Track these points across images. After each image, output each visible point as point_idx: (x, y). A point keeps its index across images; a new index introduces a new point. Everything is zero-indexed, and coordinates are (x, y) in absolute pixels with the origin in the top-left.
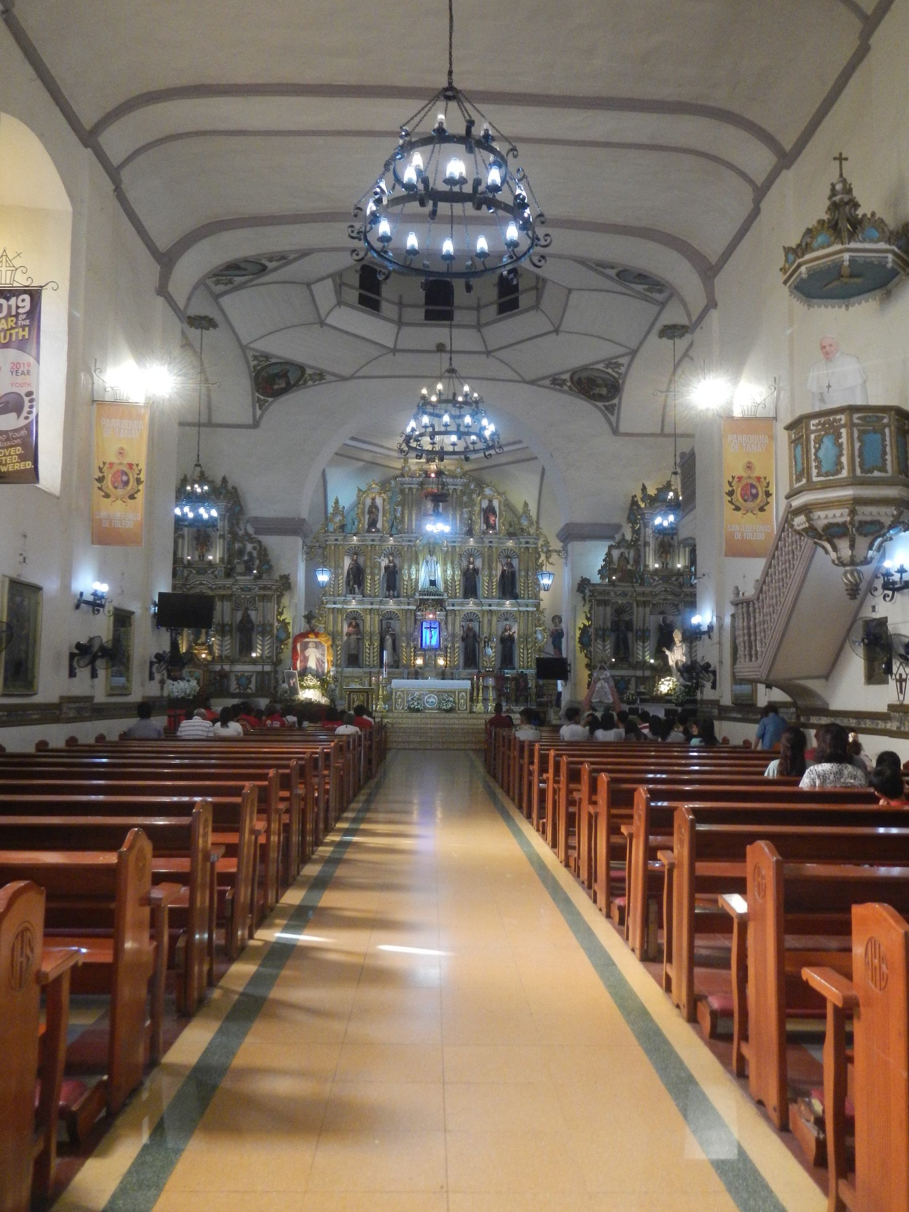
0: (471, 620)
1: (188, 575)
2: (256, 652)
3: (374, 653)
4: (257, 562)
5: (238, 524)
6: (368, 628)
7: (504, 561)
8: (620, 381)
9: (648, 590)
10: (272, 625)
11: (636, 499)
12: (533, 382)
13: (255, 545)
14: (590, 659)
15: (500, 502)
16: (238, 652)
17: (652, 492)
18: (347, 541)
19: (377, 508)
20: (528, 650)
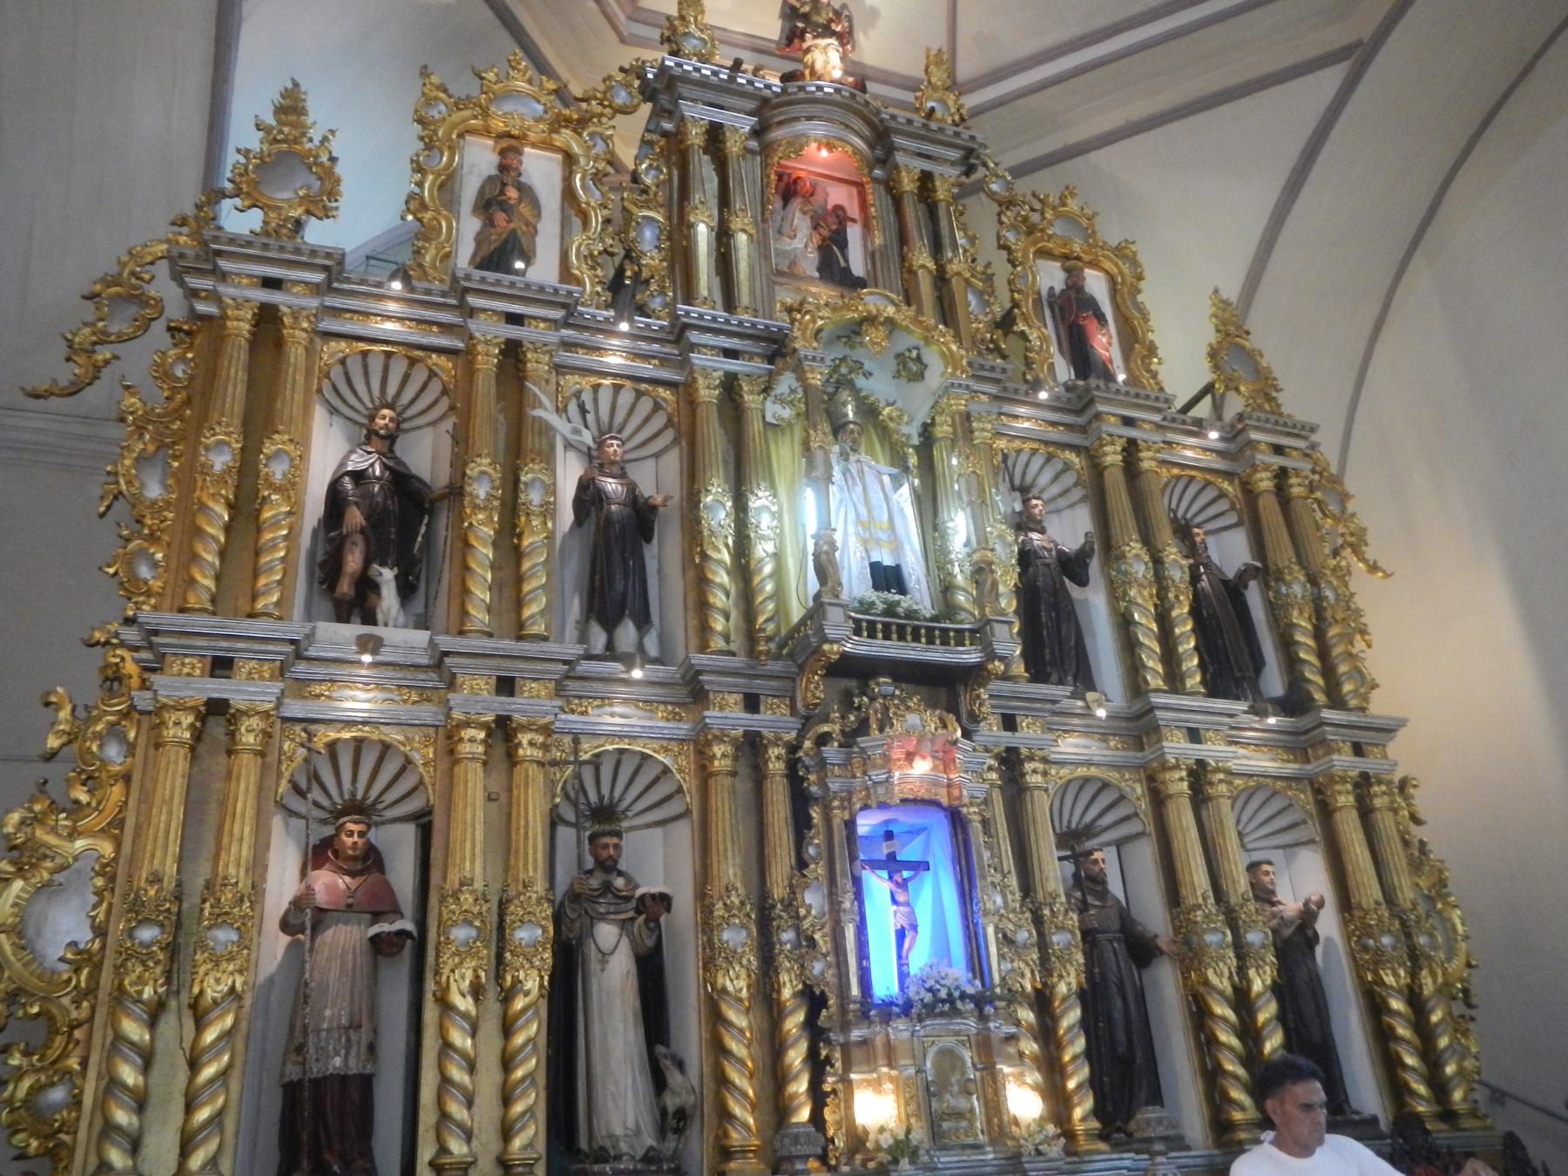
15: (1112, 280)
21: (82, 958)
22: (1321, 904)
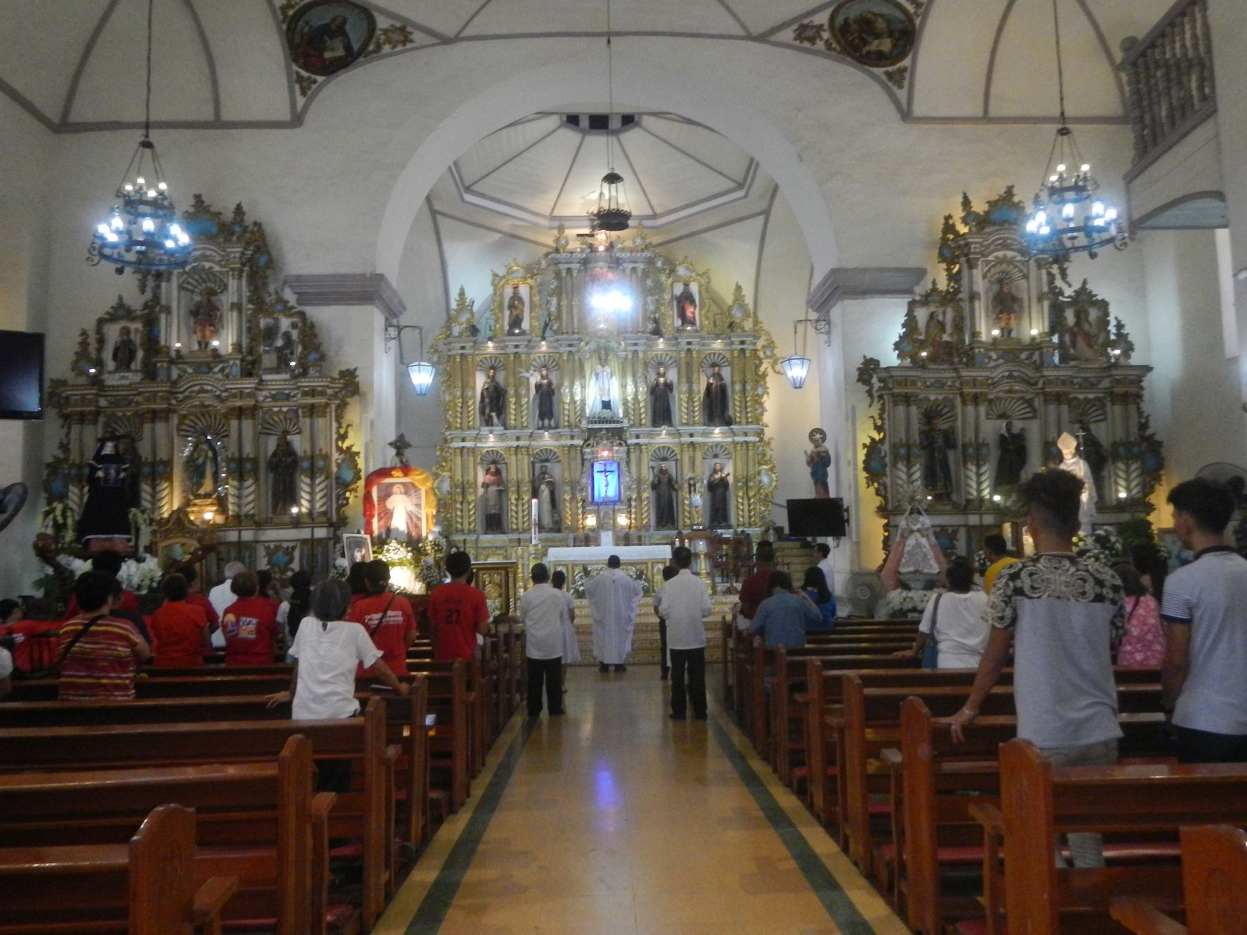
0: (664, 459)
1: (180, 377)
2: (300, 505)
3: (523, 511)
4: (300, 349)
5: (265, 285)
6: (513, 475)
7: (710, 371)
8: (918, 21)
9: (980, 374)
10: (327, 458)
11: (951, 222)
12: (762, 38)
13: (296, 319)
14: (885, 498)
15: (700, 286)
16: (270, 510)
17: (979, 207)
18: (479, 349)
19: (520, 300)
20: (749, 499)
21: (450, 493)
22: (728, 474)
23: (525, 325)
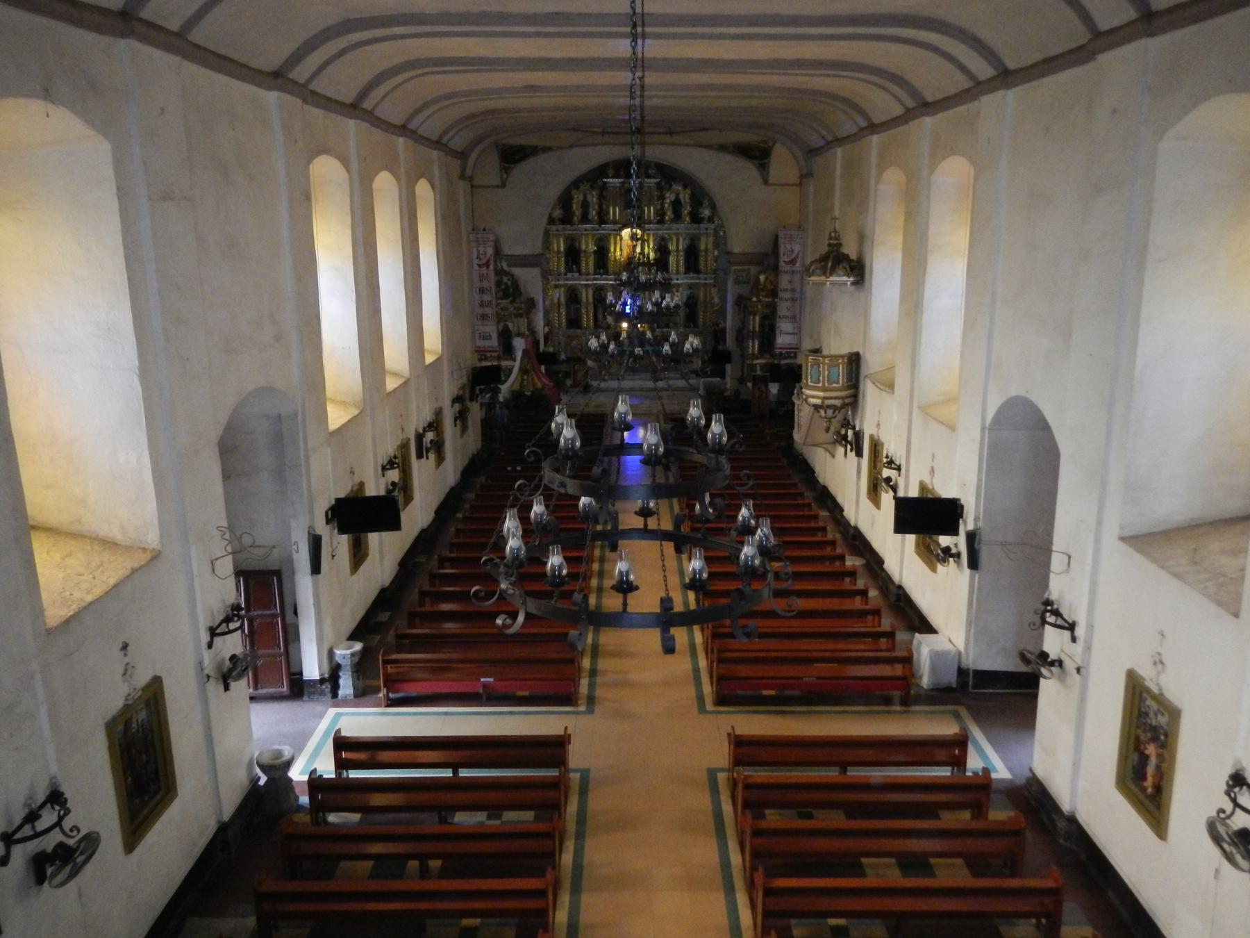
19: (587, 202)
23: (590, 217)
